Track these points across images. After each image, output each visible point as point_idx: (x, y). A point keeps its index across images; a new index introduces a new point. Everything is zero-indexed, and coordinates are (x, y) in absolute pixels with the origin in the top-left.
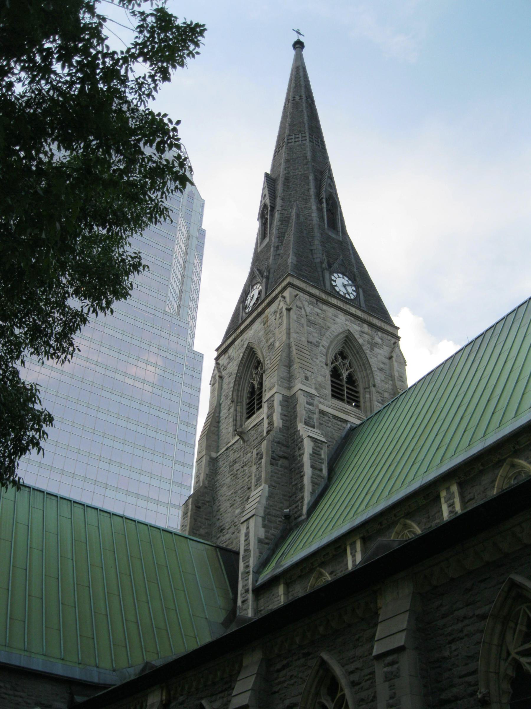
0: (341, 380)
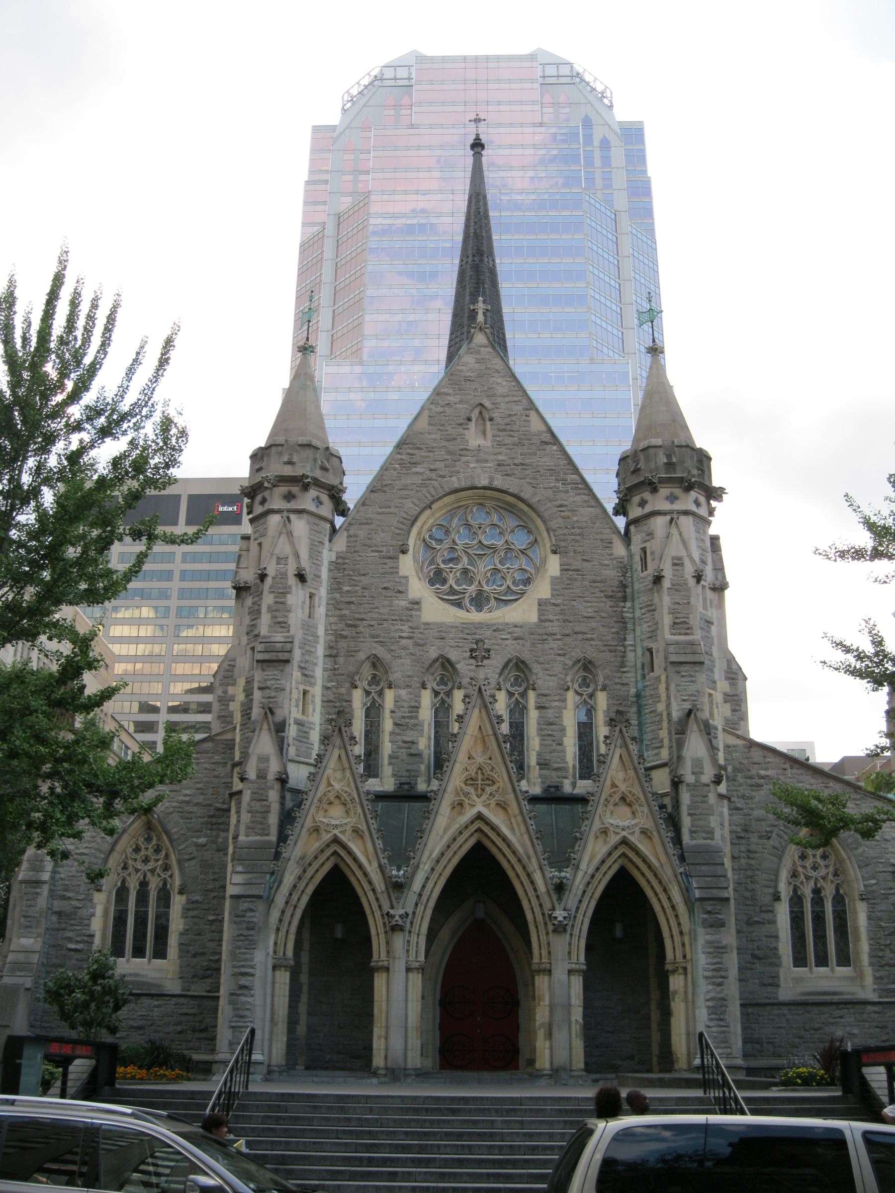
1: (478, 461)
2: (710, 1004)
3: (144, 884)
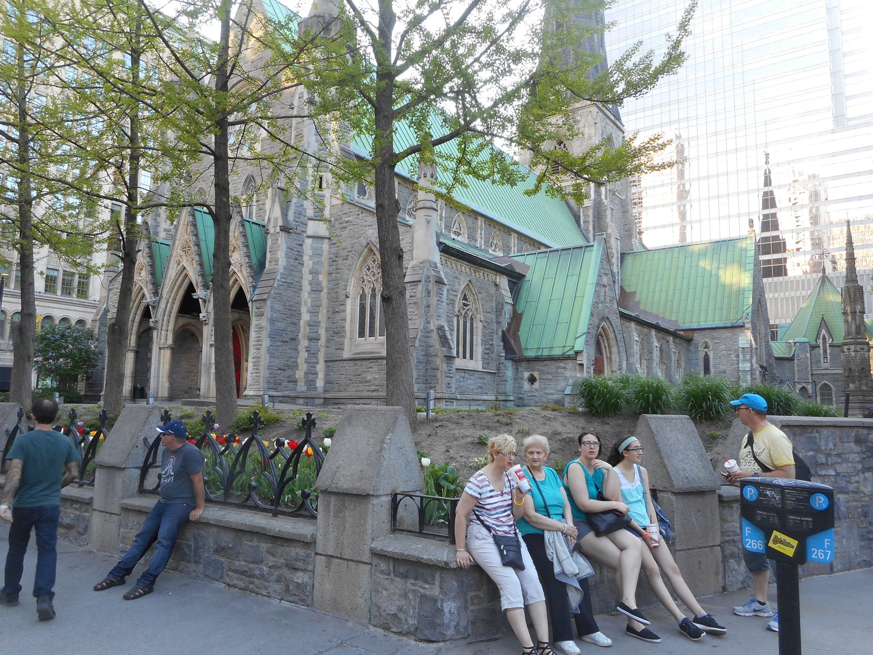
2: (254, 360)
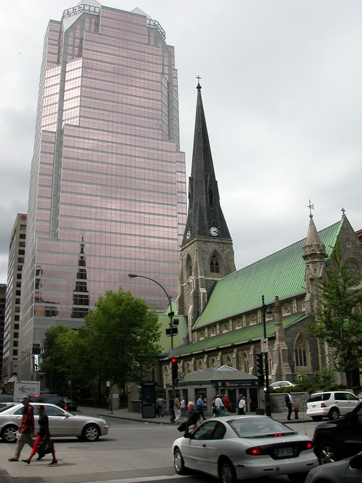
0: (214, 265)
1: (350, 251)
3: (300, 349)
